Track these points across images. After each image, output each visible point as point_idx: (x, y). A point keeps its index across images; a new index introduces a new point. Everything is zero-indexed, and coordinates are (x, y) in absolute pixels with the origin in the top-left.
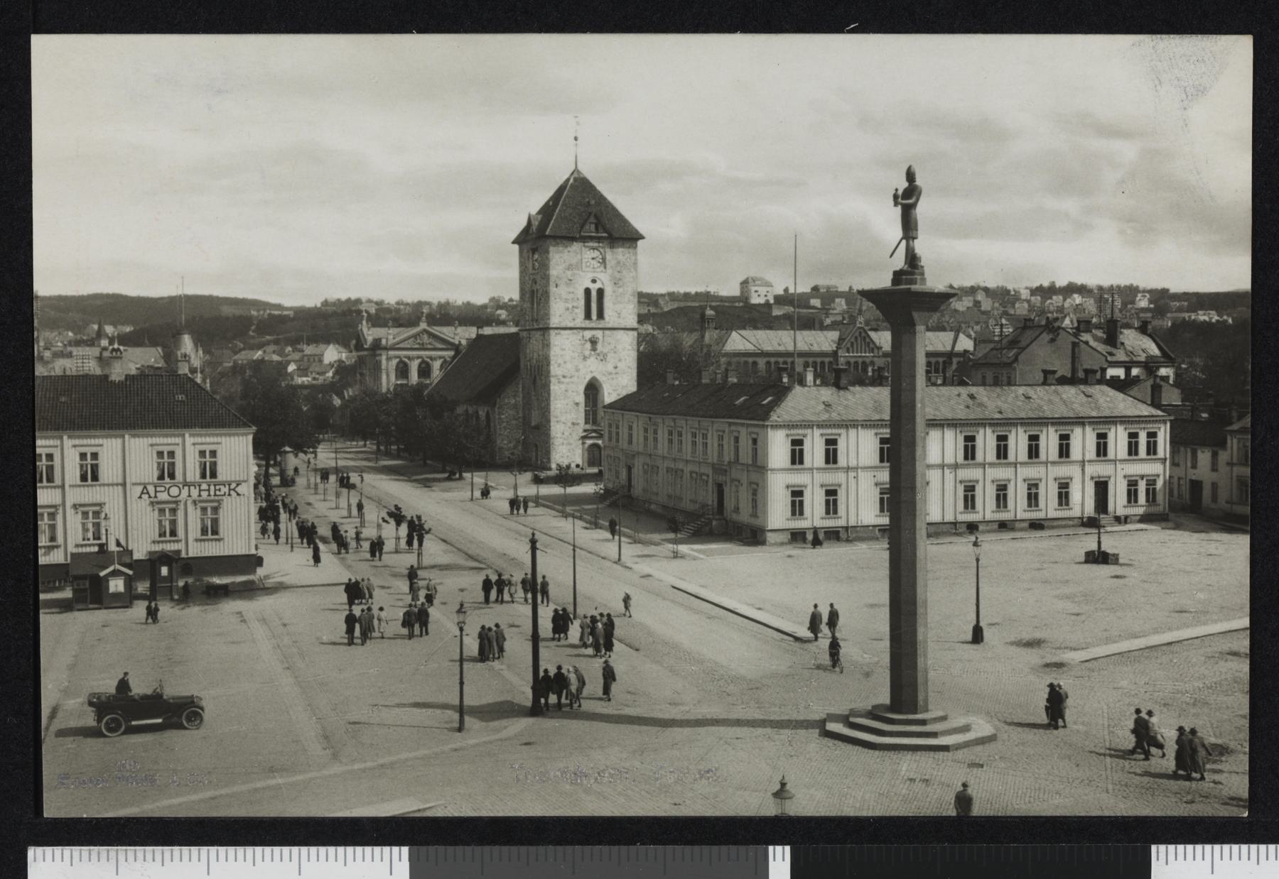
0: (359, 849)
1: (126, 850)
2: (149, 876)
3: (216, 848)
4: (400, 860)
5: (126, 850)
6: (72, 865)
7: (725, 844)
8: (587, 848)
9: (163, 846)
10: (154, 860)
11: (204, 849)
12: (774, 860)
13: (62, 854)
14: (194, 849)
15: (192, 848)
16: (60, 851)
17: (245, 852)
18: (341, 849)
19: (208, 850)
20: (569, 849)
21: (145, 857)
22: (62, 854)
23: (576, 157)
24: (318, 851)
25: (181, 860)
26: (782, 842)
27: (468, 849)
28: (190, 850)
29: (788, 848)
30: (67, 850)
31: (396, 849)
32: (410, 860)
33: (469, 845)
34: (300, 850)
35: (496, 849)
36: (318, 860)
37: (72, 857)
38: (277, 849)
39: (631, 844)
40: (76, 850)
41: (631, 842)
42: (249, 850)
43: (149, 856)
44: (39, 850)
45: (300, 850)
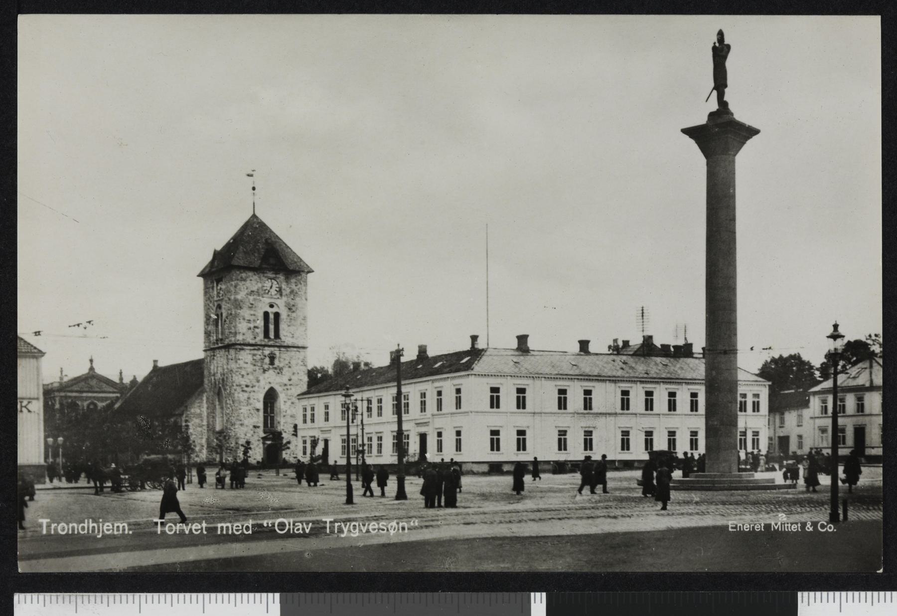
0: (245, 595)
1: (83, 595)
3: (145, 594)
4: (274, 602)
5: (83, 595)
6: (44, 606)
7: (500, 591)
8: (404, 594)
10: (102, 603)
11: (137, 595)
12: (535, 602)
13: (38, 598)
14: (130, 595)
15: (129, 594)
16: (37, 597)
17: (165, 597)
18: (232, 595)
19: (140, 595)
20: (392, 595)
21: (95, 600)
22: (38, 598)
23: (254, 203)
24: (216, 597)
25: (121, 603)
26: (540, 591)
27: (321, 595)
28: (127, 596)
29: (544, 594)
31: (271, 595)
32: (280, 603)
34: (204, 596)
35: (341, 595)
36: (216, 603)
37: (45, 601)
38: (188, 595)
41: (434, 590)
42: (169, 595)
43: (99, 600)
44: (22, 595)
45: (204, 596)
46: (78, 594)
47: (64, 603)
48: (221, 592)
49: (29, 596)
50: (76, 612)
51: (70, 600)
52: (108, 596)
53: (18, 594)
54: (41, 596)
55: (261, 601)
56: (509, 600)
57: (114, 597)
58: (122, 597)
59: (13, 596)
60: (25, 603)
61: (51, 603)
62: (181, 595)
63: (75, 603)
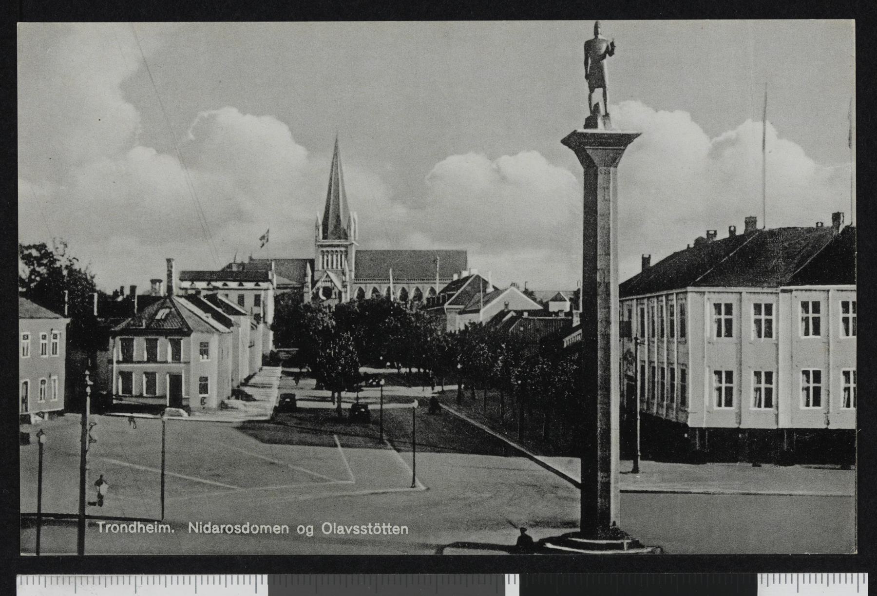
0: (235, 576)
1: (81, 577)
2: (96, 594)
3: (140, 575)
4: (262, 583)
5: (81, 577)
6: (45, 587)
7: (476, 573)
8: (386, 576)
10: (100, 584)
11: (133, 576)
12: (509, 583)
13: (39, 579)
14: (126, 577)
17: (160, 578)
18: (223, 576)
19: (136, 577)
20: (373, 576)
21: (94, 581)
22: (39, 579)
25: (118, 584)
26: (514, 572)
27: (307, 576)
29: (518, 576)
30: (42, 577)
31: (259, 576)
32: (268, 584)
34: (196, 577)
35: (325, 576)
36: (208, 584)
37: (45, 582)
38: (181, 576)
39: (414, 573)
40: (48, 577)
41: (414, 571)
42: (163, 577)
43: (96, 580)
44: (24, 577)
46: (77, 575)
50: (75, 592)
51: (69, 581)
52: (105, 577)
54: (42, 577)
56: (485, 581)
60: (27, 584)
61: (51, 584)
62: (175, 576)
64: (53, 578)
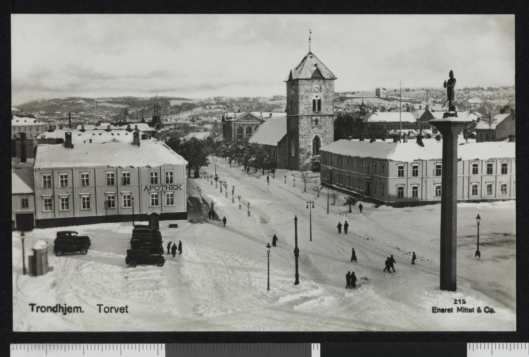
0: (145, 345)
1: (50, 345)
3: (87, 344)
4: (162, 349)
5: (50, 345)
6: (28, 351)
7: (293, 343)
8: (238, 344)
9: (65, 343)
10: (61, 349)
11: (82, 345)
12: (314, 349)
13: (24, 346)
14: (78, 345)
17: (98, 346)
18: (137, 345)
19: (84, 345)
20: (230, 344)
21: (58, 348)
22: (24, 346)
25: (73, 349)
27: (189, 344)
28: (76, 345)
29: (319, 344)
31: (160, 345)
32: (165, 349)
33: (189, 343)
34: (121, 345)
41: (255, 342)
42: (100, 345)
43: (60, 347)
44: (15, 345)
45: (121, 345)
47: (39, 349)
48: (131, 343)
49: (19, 345)
50: (47, 355)
51: (43, 347)
52: (65, 345)
53: (12, 344)
54: (26, 345)
55: (154, 348)
57: (69, 346)
58: (73, 346)
59: (10, 345)
60: (17, 349)
61: (32, 349)
63: (46, 349)
64: (33, 346)
